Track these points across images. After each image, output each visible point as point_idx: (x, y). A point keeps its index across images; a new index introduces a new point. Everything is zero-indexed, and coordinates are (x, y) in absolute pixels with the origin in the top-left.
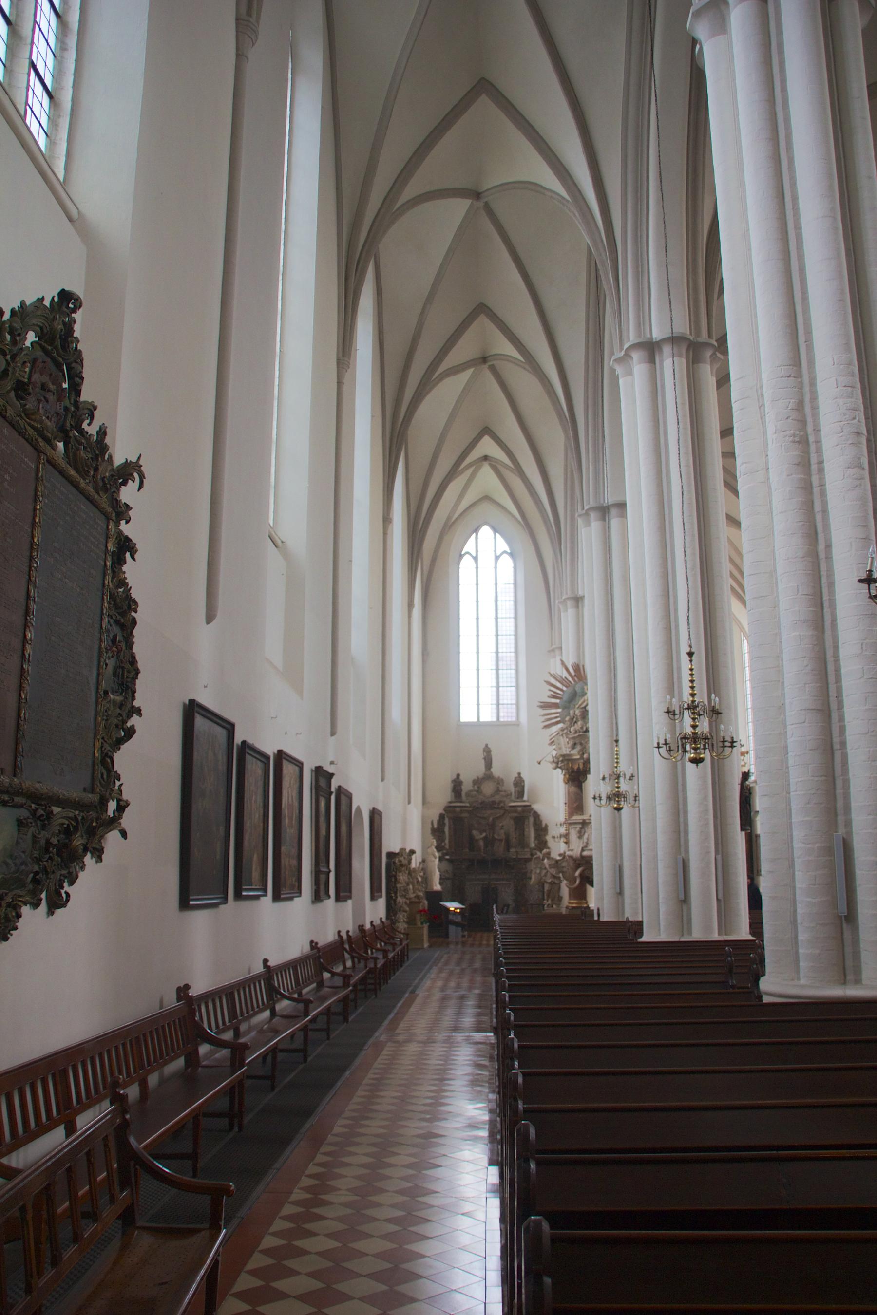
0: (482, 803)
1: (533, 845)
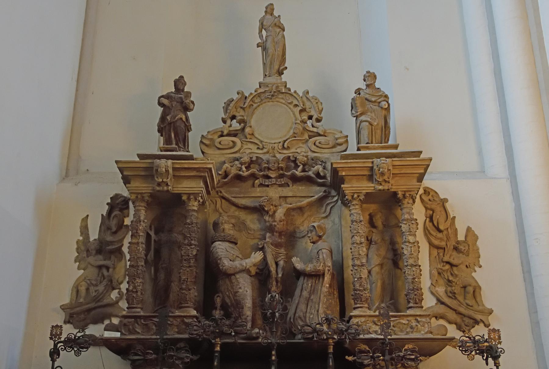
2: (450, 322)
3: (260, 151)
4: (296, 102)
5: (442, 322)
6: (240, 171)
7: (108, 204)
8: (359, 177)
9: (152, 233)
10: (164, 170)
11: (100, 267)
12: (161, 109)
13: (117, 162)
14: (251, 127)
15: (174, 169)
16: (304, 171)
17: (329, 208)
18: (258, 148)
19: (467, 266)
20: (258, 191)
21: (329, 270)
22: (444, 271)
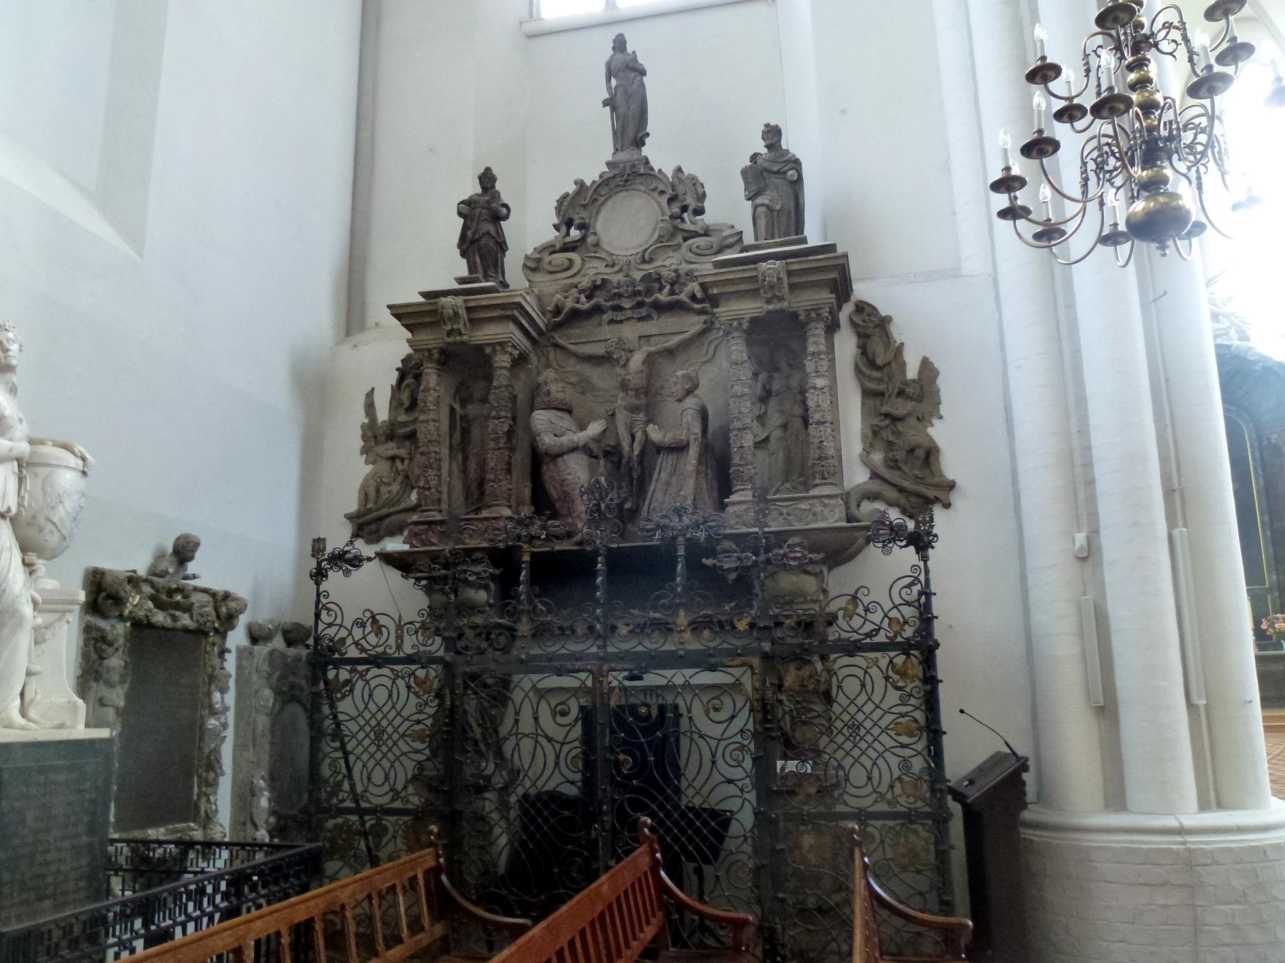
0: (592, 291)
1: (857, 476)
2: (891, 504)
3: (609, 270)
4: (661, 187)
5: (880, 506)
6: (578, 302)
7: (397, 369)
8: (740, 295)
9: (457, 406)
10: (451, 311)
11: (393, 459)
12: (462, 220)
13: (389, 307)
14: (595, 234)
15: (469, 310)
16: (672, 293)
17: (712, 347)
18: (607, 266)
19: (918, 418)
20: (607, 332)
21: (696, 439)
22: (882, 428)
